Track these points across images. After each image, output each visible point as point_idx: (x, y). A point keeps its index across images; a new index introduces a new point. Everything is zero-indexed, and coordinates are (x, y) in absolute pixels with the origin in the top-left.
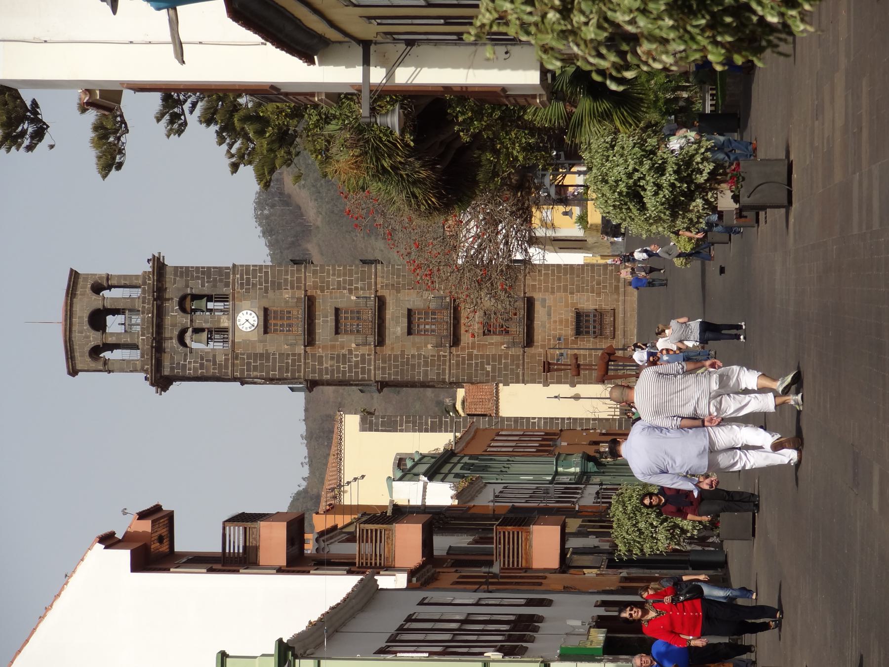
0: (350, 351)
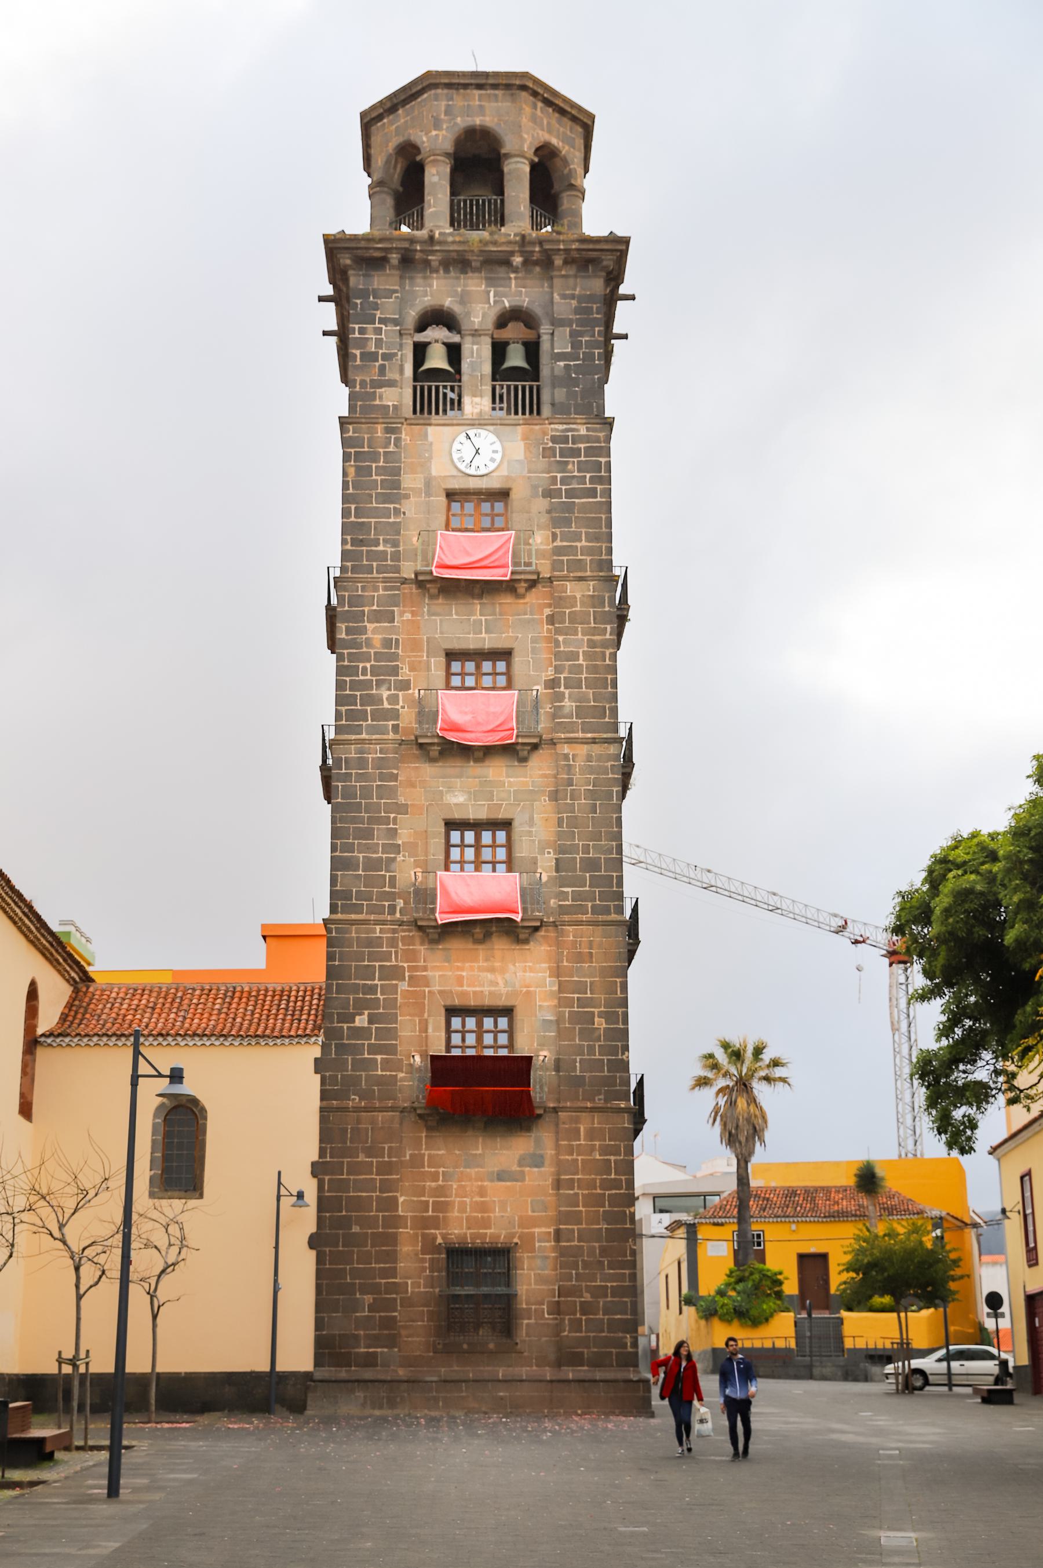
0: (405, 685)
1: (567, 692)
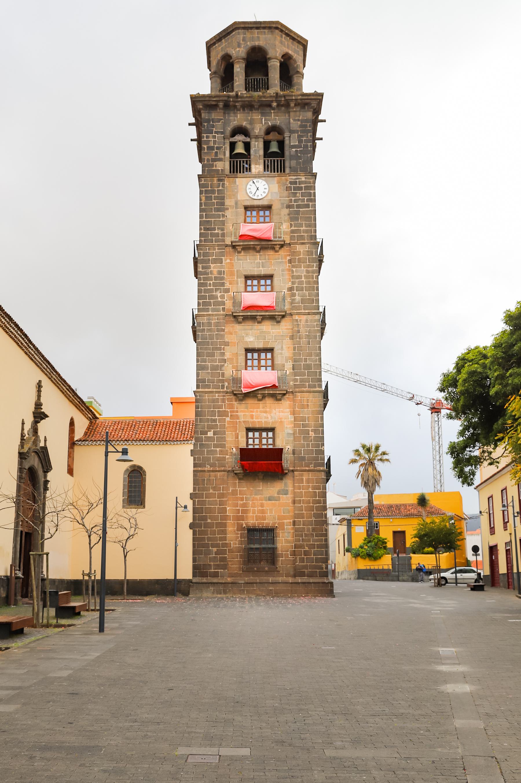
0: (227, 291)
1: (297, 292)
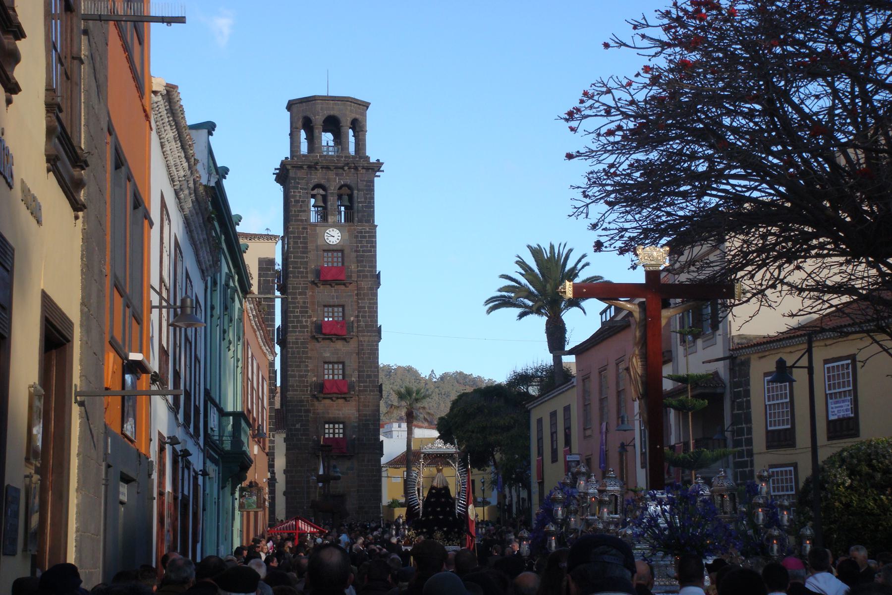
0: (310, 317)
